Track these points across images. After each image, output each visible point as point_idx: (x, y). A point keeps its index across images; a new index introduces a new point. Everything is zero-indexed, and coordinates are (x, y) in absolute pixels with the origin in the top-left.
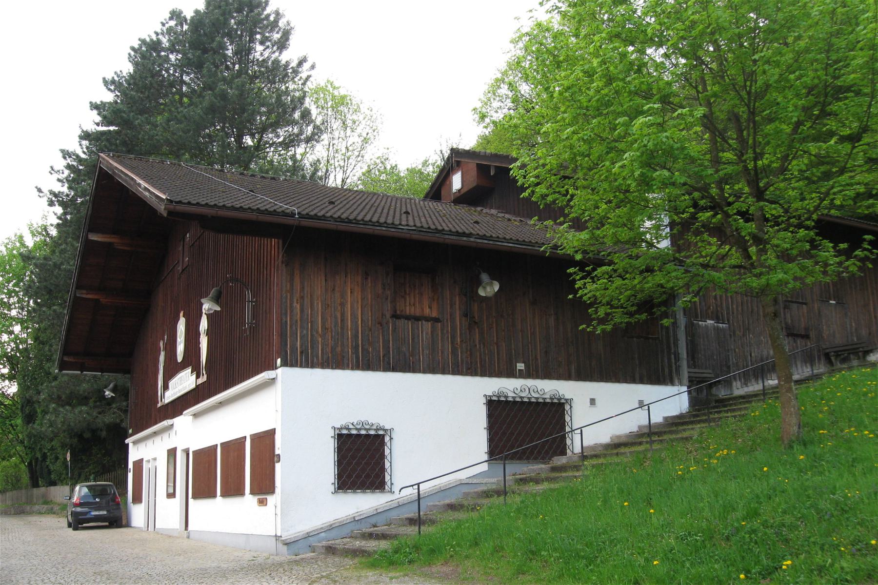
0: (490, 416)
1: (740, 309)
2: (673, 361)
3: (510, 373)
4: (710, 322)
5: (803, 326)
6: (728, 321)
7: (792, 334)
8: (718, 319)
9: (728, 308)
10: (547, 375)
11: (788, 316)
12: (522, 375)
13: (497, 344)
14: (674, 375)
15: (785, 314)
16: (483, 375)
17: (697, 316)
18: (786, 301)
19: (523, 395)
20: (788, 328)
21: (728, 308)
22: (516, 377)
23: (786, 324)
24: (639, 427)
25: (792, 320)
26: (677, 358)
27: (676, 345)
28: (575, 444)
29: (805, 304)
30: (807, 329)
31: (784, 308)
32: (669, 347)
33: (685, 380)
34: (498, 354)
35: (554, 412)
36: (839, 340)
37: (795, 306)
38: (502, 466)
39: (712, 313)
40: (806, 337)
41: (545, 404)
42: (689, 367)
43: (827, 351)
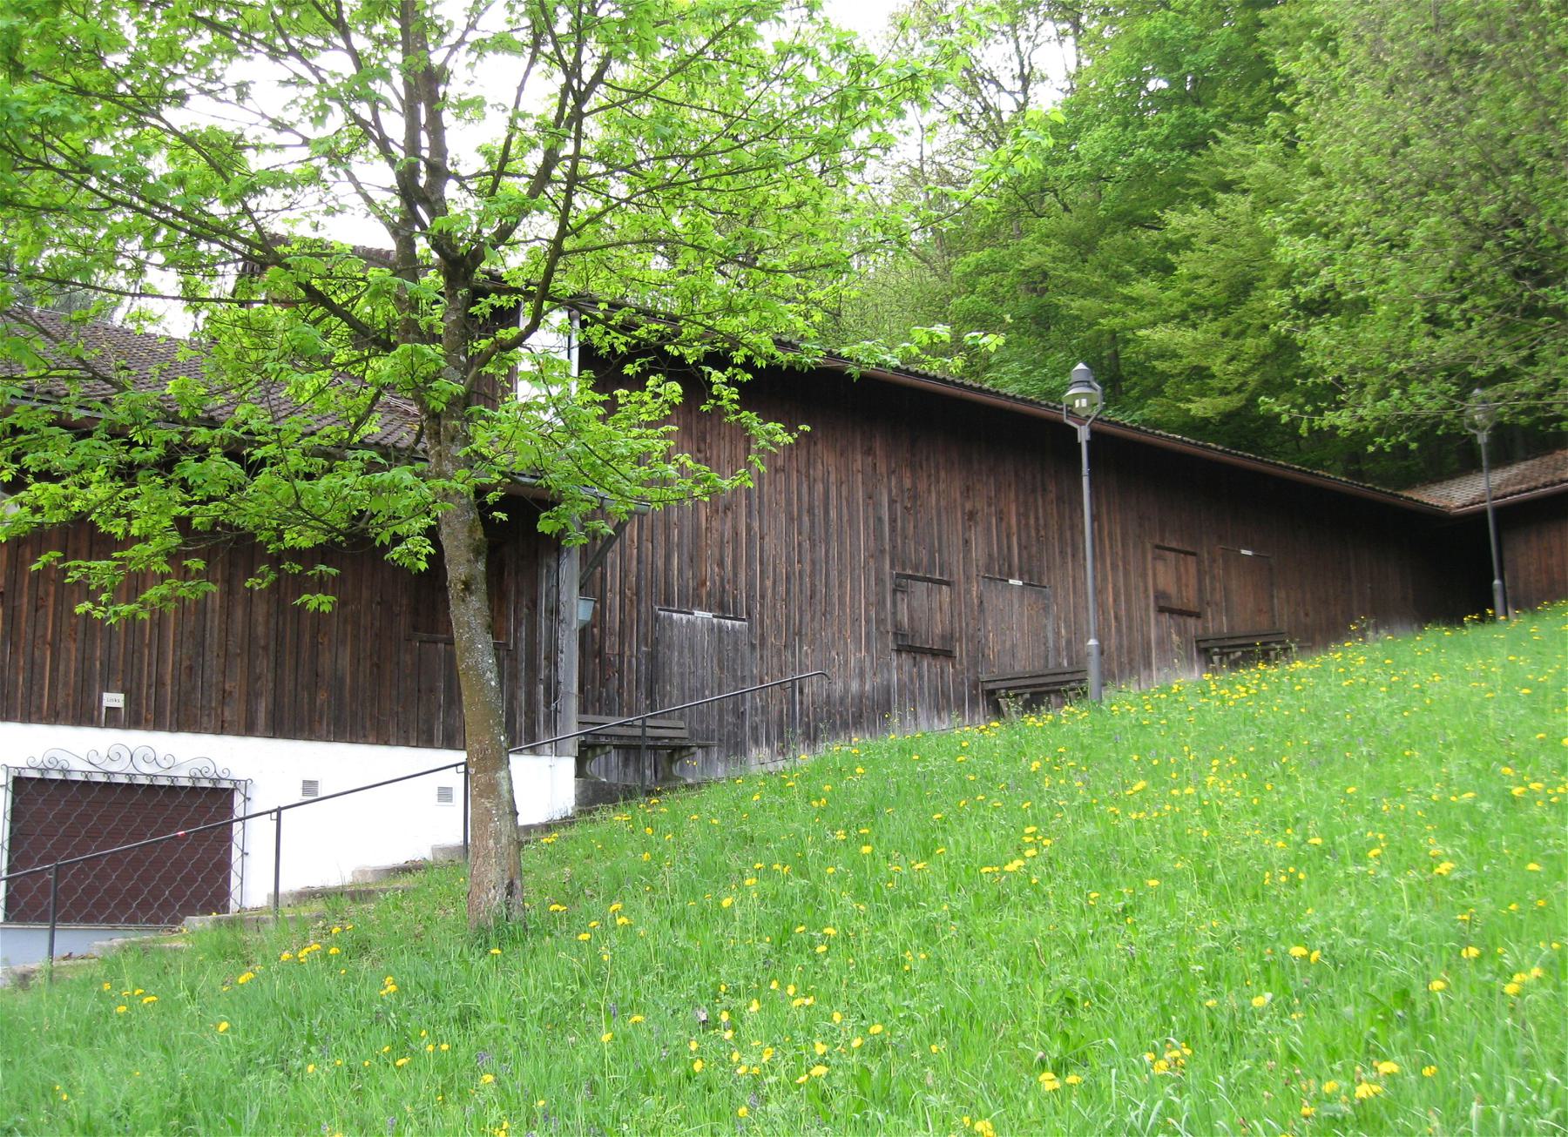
0: (16, 815)
1: (782, 589)
2: (541, 697)
3: (84, 714)
4: (701, 615)
5: (938, 630)
6: (749, 614)
7: (908, 647)
8: (722, 609)
9: (750, 585)
10: (185, 721)
11: (903, 609)
12: (113, 719)
13: (52, 645)
14: (541, 729)
15: (894, 604)
16: (27, 718)
17: (668, 601)
18: (898, 576)
19: (113, 768)
20: (898, 633)
21: (750, 585)
22: (98, 725)
23: (897, 626)
24: (435, 850)
25: (911, 619)
26: (553, 693)
27: (553, 661)
28: (252, 884)
29: (948, 584)
30: (949, 637)
31: (895, 591)
32: (532, 667)
33: (572, 746)
34: (54, 669)
35: (212, 804)
36: (1024, 663)
37: (921, 587)
38: (46, 936)
39: (709, 594)
40: (948, 654)
41: (173, 790)
42: (583, 709)
43: (991, 686)
